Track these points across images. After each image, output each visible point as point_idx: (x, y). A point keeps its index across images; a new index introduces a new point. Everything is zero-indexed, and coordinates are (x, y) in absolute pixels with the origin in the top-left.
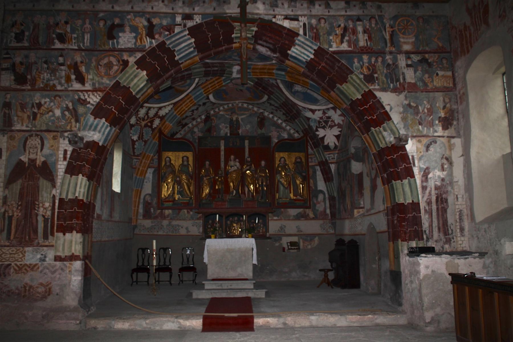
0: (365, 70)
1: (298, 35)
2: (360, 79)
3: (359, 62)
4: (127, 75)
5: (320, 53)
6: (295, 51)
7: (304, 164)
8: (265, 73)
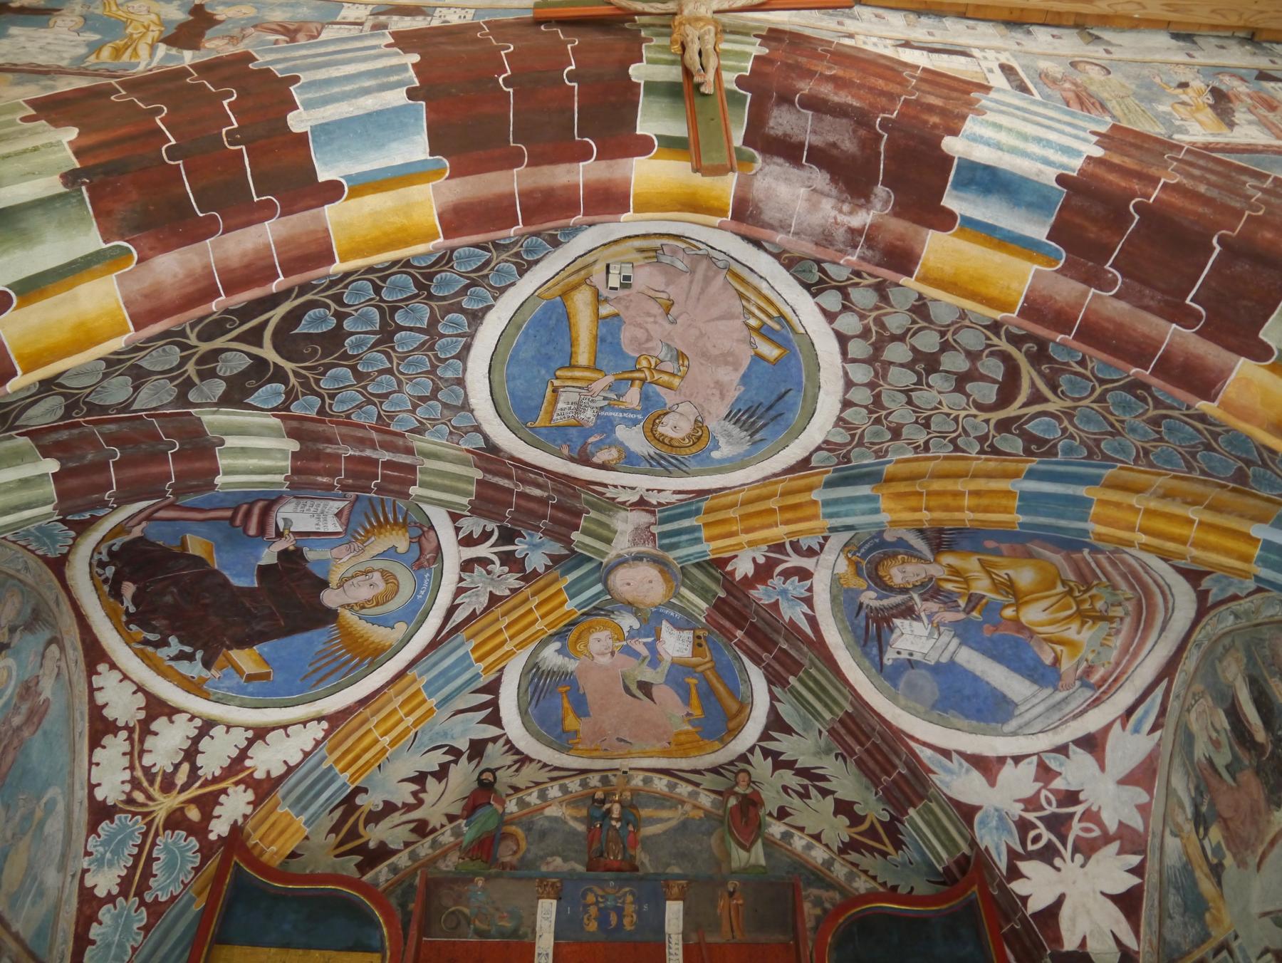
1: (986, 89)
6: (988, 133)
8: (772, 511)
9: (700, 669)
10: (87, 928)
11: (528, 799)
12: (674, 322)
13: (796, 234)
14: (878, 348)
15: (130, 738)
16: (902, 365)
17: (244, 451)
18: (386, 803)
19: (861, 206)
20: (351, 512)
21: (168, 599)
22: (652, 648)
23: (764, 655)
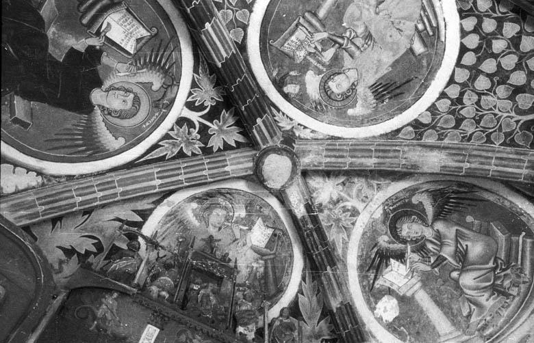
12: (377, 14)
14: (480, 60)
20: (147, 42)
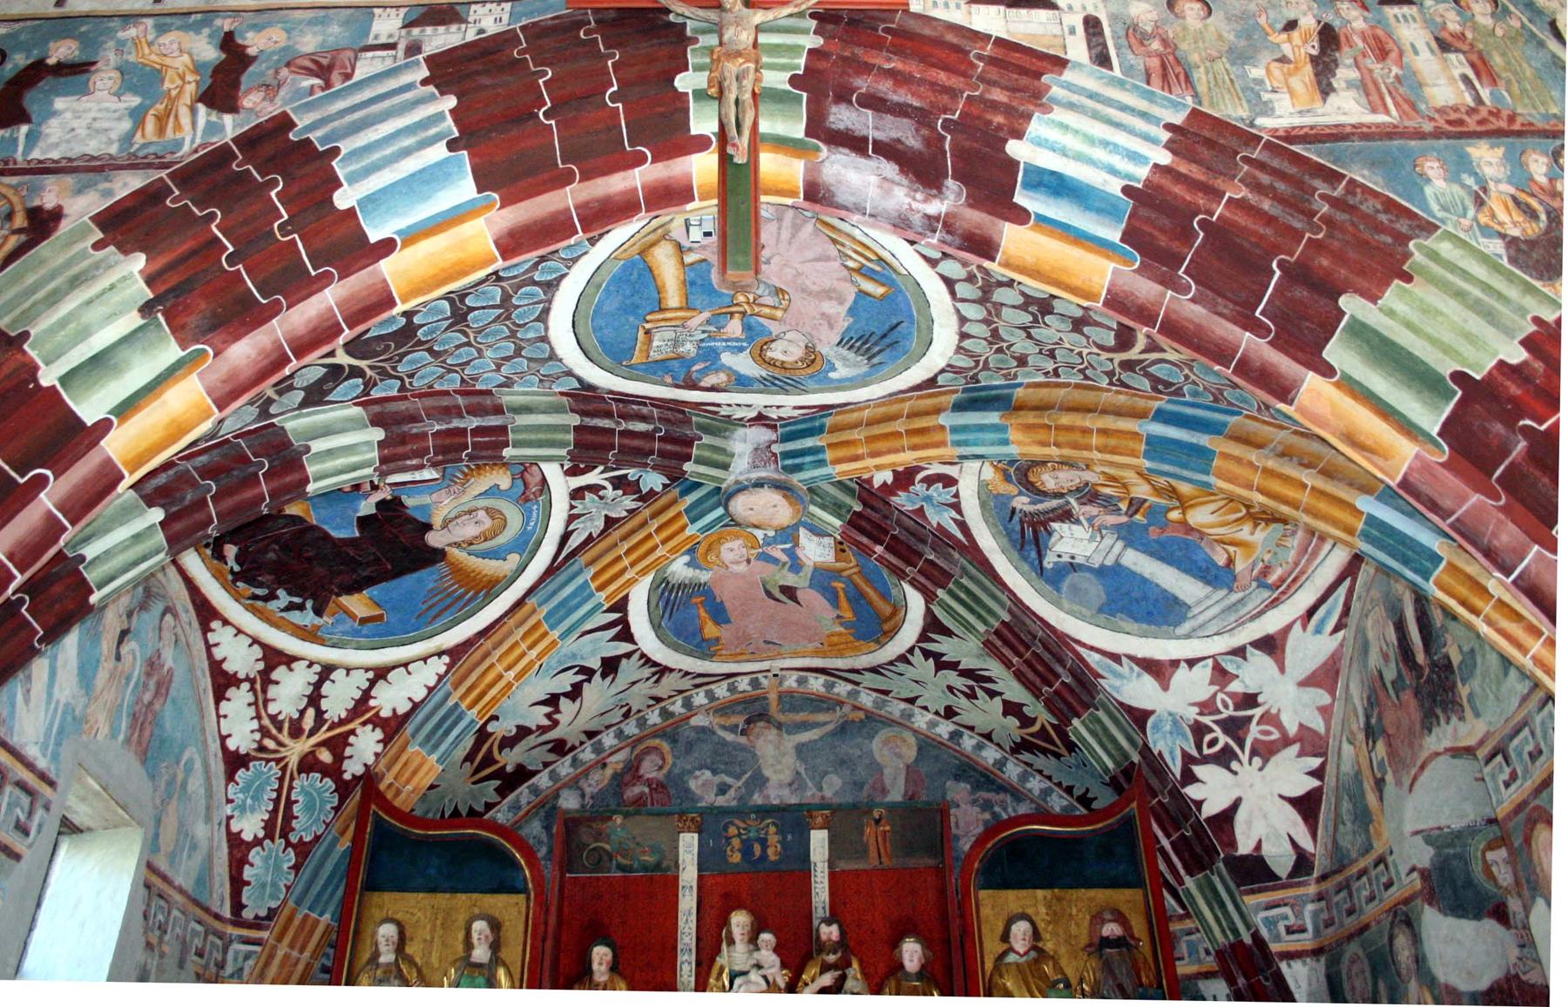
0: (1502, 216)
1: (1060, 63)
2: (1484, 258)
3: (1453, 178)
4: (31, 279)
5: (1203, 139)
6: (1054, 135)
7: (1144, 945)
8: (897, 435)
9: (845, 574)
10: (241, 873)
11: (671, 708)
13: (872, 215)
15: (252, 689)
16: (1014, 307)
17: (330, 453)
18: (518, 727)
19: (935, 196)
21: (271, 555)
22: (791, 554)
23: (908, 569)
